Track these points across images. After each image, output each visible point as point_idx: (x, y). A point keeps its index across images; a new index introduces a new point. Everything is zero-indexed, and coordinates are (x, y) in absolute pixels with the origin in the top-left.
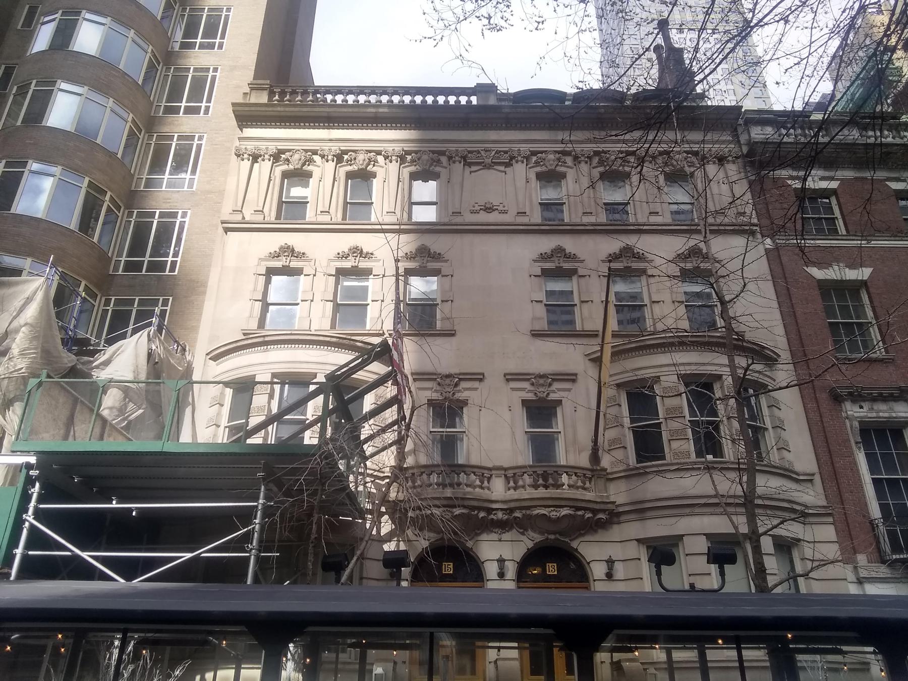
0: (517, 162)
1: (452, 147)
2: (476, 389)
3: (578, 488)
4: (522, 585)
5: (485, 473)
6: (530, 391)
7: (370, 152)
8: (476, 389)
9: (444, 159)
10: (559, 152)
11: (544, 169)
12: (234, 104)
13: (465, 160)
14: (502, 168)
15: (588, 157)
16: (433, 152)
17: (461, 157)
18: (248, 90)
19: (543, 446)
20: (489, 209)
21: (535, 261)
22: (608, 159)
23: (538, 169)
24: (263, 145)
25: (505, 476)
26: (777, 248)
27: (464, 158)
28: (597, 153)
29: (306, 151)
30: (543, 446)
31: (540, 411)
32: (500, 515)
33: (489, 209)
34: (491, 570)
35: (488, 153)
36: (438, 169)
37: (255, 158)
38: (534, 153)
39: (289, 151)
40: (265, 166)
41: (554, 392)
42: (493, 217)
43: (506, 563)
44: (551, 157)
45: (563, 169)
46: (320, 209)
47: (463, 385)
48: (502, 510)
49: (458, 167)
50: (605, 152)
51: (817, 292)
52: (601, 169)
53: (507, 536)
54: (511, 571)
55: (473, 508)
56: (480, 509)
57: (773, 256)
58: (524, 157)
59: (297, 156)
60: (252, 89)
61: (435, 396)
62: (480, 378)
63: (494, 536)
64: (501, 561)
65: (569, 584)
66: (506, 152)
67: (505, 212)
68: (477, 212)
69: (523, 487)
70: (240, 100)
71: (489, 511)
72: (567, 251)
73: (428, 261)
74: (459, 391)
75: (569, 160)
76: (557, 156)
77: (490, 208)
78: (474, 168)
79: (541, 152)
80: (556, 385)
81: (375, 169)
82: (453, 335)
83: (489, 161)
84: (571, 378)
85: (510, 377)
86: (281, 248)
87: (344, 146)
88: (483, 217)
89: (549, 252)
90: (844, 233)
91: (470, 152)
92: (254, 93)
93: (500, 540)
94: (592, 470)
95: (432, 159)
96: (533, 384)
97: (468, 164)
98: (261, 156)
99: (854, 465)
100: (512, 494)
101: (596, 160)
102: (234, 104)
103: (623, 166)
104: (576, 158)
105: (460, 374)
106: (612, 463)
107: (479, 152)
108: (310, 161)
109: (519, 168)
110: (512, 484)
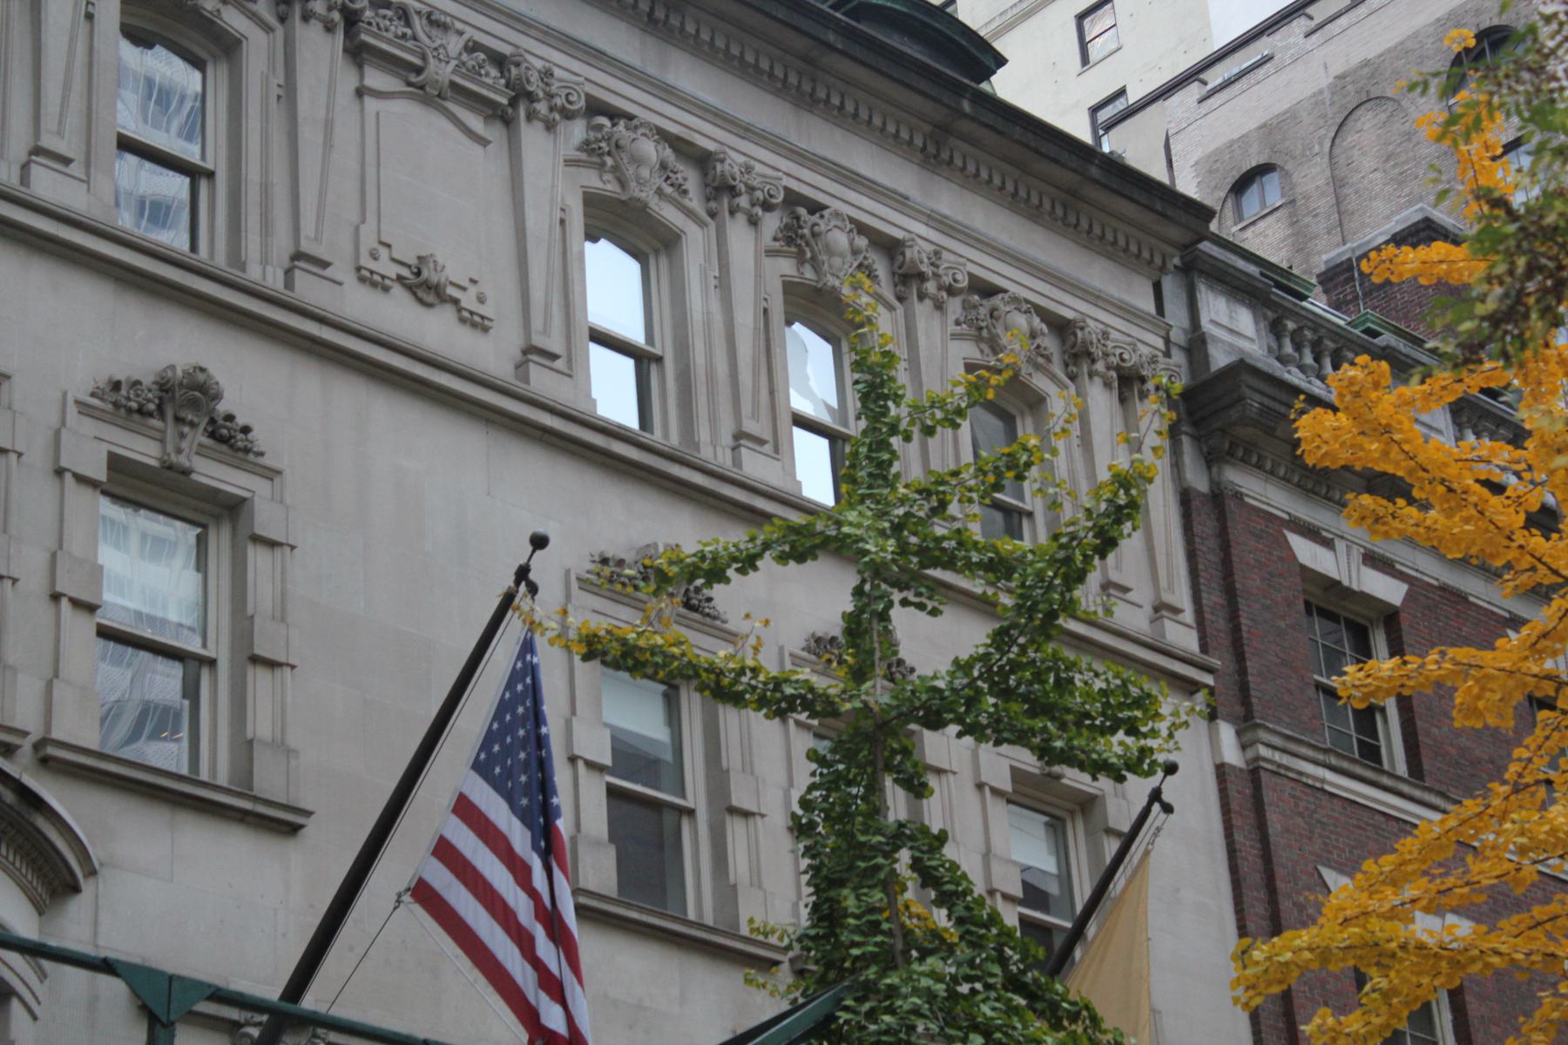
0: (531, 116)
11: (611, 187)
14: (475, 122)
20: (424, 287)
28: (793, 199)
33: (424, 287)
35: (439, 38)
38: (595, 108)
42: (432, 330)
44: (649, 149)
45: (669, 214)
50: (816, 208)
57: (1244, 796)
66: (499, 61)
67: (479, 324)
76: (668, 153)
78: (376, 79)
79: (615, 115)
83: (441, 72)
88: (397, 316)
90: (1402, 769)
97: (358, 53)
109: (546, 155)
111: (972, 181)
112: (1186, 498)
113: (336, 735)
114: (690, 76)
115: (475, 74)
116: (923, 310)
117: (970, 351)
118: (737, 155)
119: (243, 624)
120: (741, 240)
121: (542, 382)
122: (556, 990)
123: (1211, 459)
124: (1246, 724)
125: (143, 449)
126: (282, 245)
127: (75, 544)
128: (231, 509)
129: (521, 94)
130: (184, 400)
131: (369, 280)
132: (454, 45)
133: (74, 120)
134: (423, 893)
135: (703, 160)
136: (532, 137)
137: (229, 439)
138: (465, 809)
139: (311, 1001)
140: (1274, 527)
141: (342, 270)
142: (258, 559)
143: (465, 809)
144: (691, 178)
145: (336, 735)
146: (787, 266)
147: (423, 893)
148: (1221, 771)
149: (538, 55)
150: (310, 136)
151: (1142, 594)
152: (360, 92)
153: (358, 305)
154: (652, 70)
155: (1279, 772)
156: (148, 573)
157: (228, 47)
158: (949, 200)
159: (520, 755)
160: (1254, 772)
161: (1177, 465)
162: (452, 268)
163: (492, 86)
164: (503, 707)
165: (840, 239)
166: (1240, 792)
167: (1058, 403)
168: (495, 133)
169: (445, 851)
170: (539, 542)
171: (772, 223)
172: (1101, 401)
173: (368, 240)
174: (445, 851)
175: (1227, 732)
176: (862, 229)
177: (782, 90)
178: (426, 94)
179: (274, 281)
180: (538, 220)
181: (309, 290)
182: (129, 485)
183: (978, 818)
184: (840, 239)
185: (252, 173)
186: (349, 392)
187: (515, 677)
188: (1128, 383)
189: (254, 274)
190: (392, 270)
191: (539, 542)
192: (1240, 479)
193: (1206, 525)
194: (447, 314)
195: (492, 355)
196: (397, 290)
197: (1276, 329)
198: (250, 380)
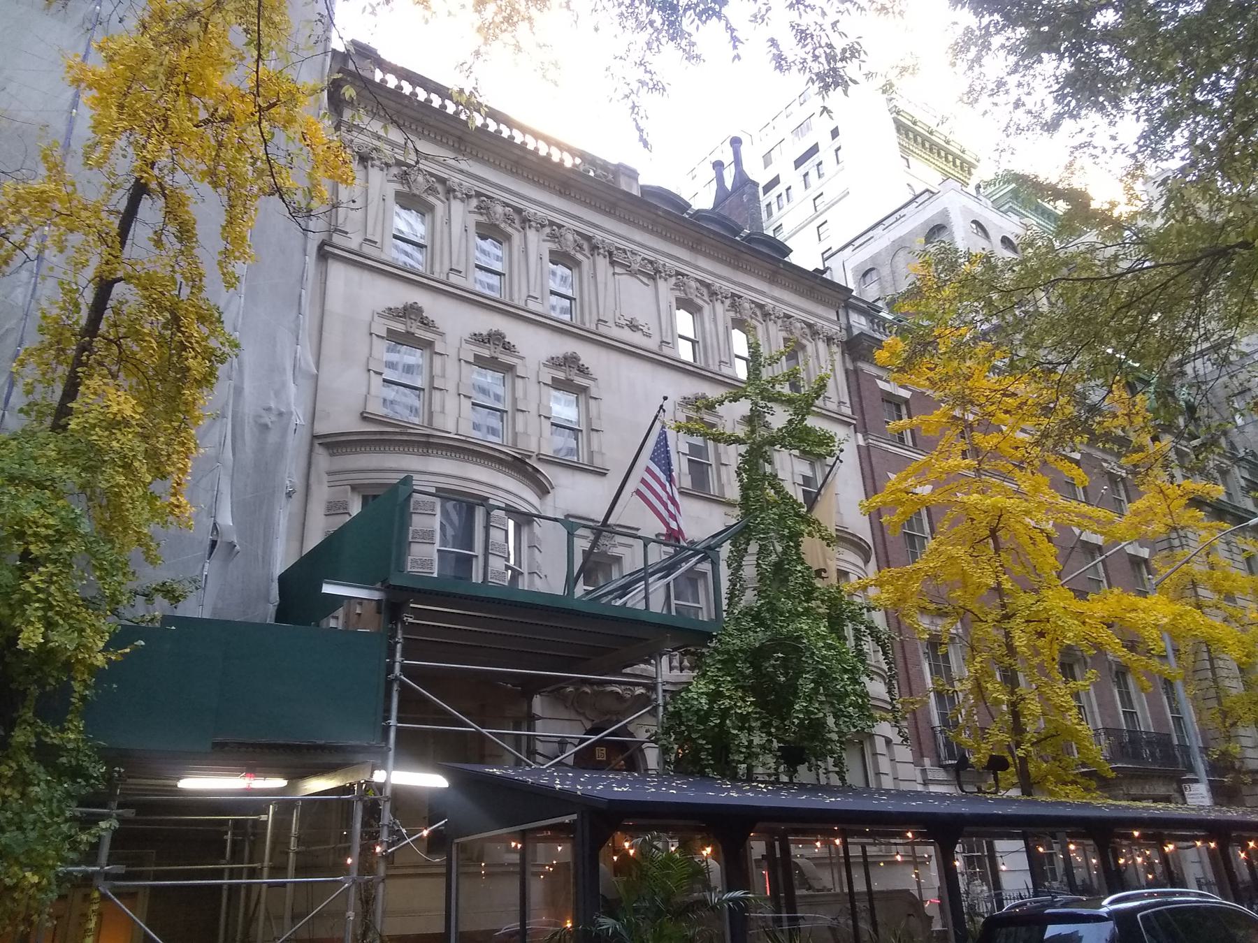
2: (630, 546)
7: (508, 205)
8: (630, 546)
11: (682, 295)
14: (645, 280)
16: (579, 233)
20: (633, 327)
27: (611, 254)
28: (733, 295)
29: (432, 175)
33: (633, 327)
36: (579, 256)
38: (678, 273)
42: (636, 338)
44: (693, 284)
45: (700, 302)
47: (619, 539)
49: (602, 263)
50: (740, 297)
51: (1128, 564)
57: (865, 454)
66: (651, 262)
67: (649, 336)
74: (614, 546)
77: (636, 327)
78: (618, 270)
79: (683, 275)
81: (509, 230)
82: (603, 474)
83: (636, 267)
91: (618, 249)
97: (613, 263)
98: (373, 159)
99: (921, 672)
107: (625, 251)
108: (431, 190)
109: (665, 289)
111: (784, 287)
112: (847, 371)
113: (615, 449)
114: (703, 262)
115: (644, 266)
116: (770, 324)
117: (784, 334)
118: (718, 284)
119: (589, 420)
120: (718, 305)
121: (666, 351)
122: (674, 518)
123: (854, 360)
124: (865, 434)
125: (561, 375)
126: (595, 318)
127: (544, 401)
128: (583, 390)
129: (657, 271)
130: (570, 361)
132: (639, 259)
133: (538, 288)
134: (638, 492)
135: (708, 286)
136: (661, 283)
137: (583, 371)
138: (648, 470)
139: (610, 521)
140: (873, 378)
141: (611, 323)
142: (592, 402)
143: (648, 470)
144: (705, 291)
145: (615, 449)
146: (732, 314)
147: (638, 492)
148: (858, 447)
149: (662, 260)
150: (601, 286)
151: (835, 399)
153: (615, 332)
154: (693, 262)
155: (875, 447)
156: (564, 408)
157: (578, 264)
158: (777, 292)
159: (662, 456)
160: (868, 447)
161: (844, 362)
162: (641, 321)
163: (649, 269)
164: (657, 443)
165: (747, 305)
166: (864, 453)
167: (810, 347)
168: (651, 283)
169: (643, 481)
170: (665, 398)
171: (728, 302)
172: (822, 346)
173: (618, 315)
174: (643, 481)
175: (860, 436)
176: (753, 302)
177: (729, 264)
178: (632, 273)
179: (593, 328)
180: (663, 306)
181: (603, 329)
182: (557, 385)
183: (789, 468)
184: (747, 305)
185: (586, 298)
186: (615, 357)
187: (660, 435)
188: (829, 340)
189: (587, 326)
191: (665, 398)
192: (860, 364)
193: (853, 379)
195: (652, 344)
197: (872, 322)
198: (588, 355)
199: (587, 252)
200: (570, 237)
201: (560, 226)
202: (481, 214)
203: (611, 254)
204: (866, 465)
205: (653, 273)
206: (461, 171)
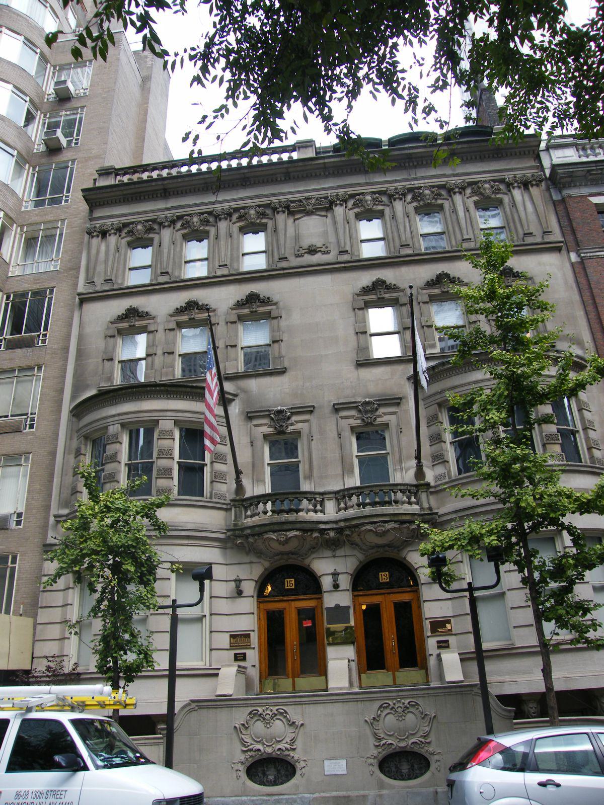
0: (336, 205)
1: (276, 200)
3: (403, 503)
4: (357, 593)
5: (318, 499)
6: (357, 418)
9: (269, 212)
10: (375, 193)
12: (83, 190)
13: (288, 210)
14: (323, 213)
15: (402, 194)
17: (285, 207)
18: (96, 176)
19: (374, 467)
20: (312, 251)
21: (358, 295)
22: (421, 194)
23: (357, 210)
24: (109, 222)
25: (336, 498)
26: (582, 261)
30: (374, 467)
31: (370, 434)
32: (332, 534)
33: (312, 251)
34: (327, 582)
37: (104, 234)
39: (132, 223)
40: (112, 239)
41: (380, 416)
42: (317, 258)
43: (340, 576)
46: (159, 272)
48: (333, 529)
49: (281, 218)
52: (415, 204)
53: (340, 552)
54: (345, 582)
55: (305, 531)
56: (312, 530)
58: (343, 201)
59: (140, 227)
60: (100, 175)
61: (270, 430)
62: (310, 410)
63: (328, 553)
64: (335, 575)
65: (400, 590)
66: (326, 198)
67: (328, 252)
68: (301, 256)
69: (352, 507)
70: (90, 185)
71: (322, 532)
72: (388, 283)
73: (259, 306)
75: (385, 199)
80: (382, 410)
84: (397, 401)
85: (337, 409)
86: (128, 310)
87: (178, 212)
88: (309, 259)
89: (370, 285)
92: (102, 178)
93: (334, 557)
94: (416, 486)
95: (258, 213)
96: (360, 411)
97: (291, 213)
98: (109, 231)
100: (343, 514)
101: (409, 197)
102: (83, 190)
103: (436, 199)
104: (391, 197)
105: (292, 408)
106: (437, 478)
107: (300, 201)
108: (150, 230)
110: (342, 505)
115: (319, 204)
131: (298, 256)
148: (572, 265)
152: (295, 220)
153: (294, 262)
165: (427, 192)
173: (297, 248)
178: (309, 213)
190: (304, 251)
192: (566, 192)
194: (319, 254)
196: (306, 255)
199: (271, 216)
200: (252, 212)
201: (244, 208)
202: (185, 228)
203: (288, 207)
204: (582, 280)
205: (327, 206)
206: (168, 209)
